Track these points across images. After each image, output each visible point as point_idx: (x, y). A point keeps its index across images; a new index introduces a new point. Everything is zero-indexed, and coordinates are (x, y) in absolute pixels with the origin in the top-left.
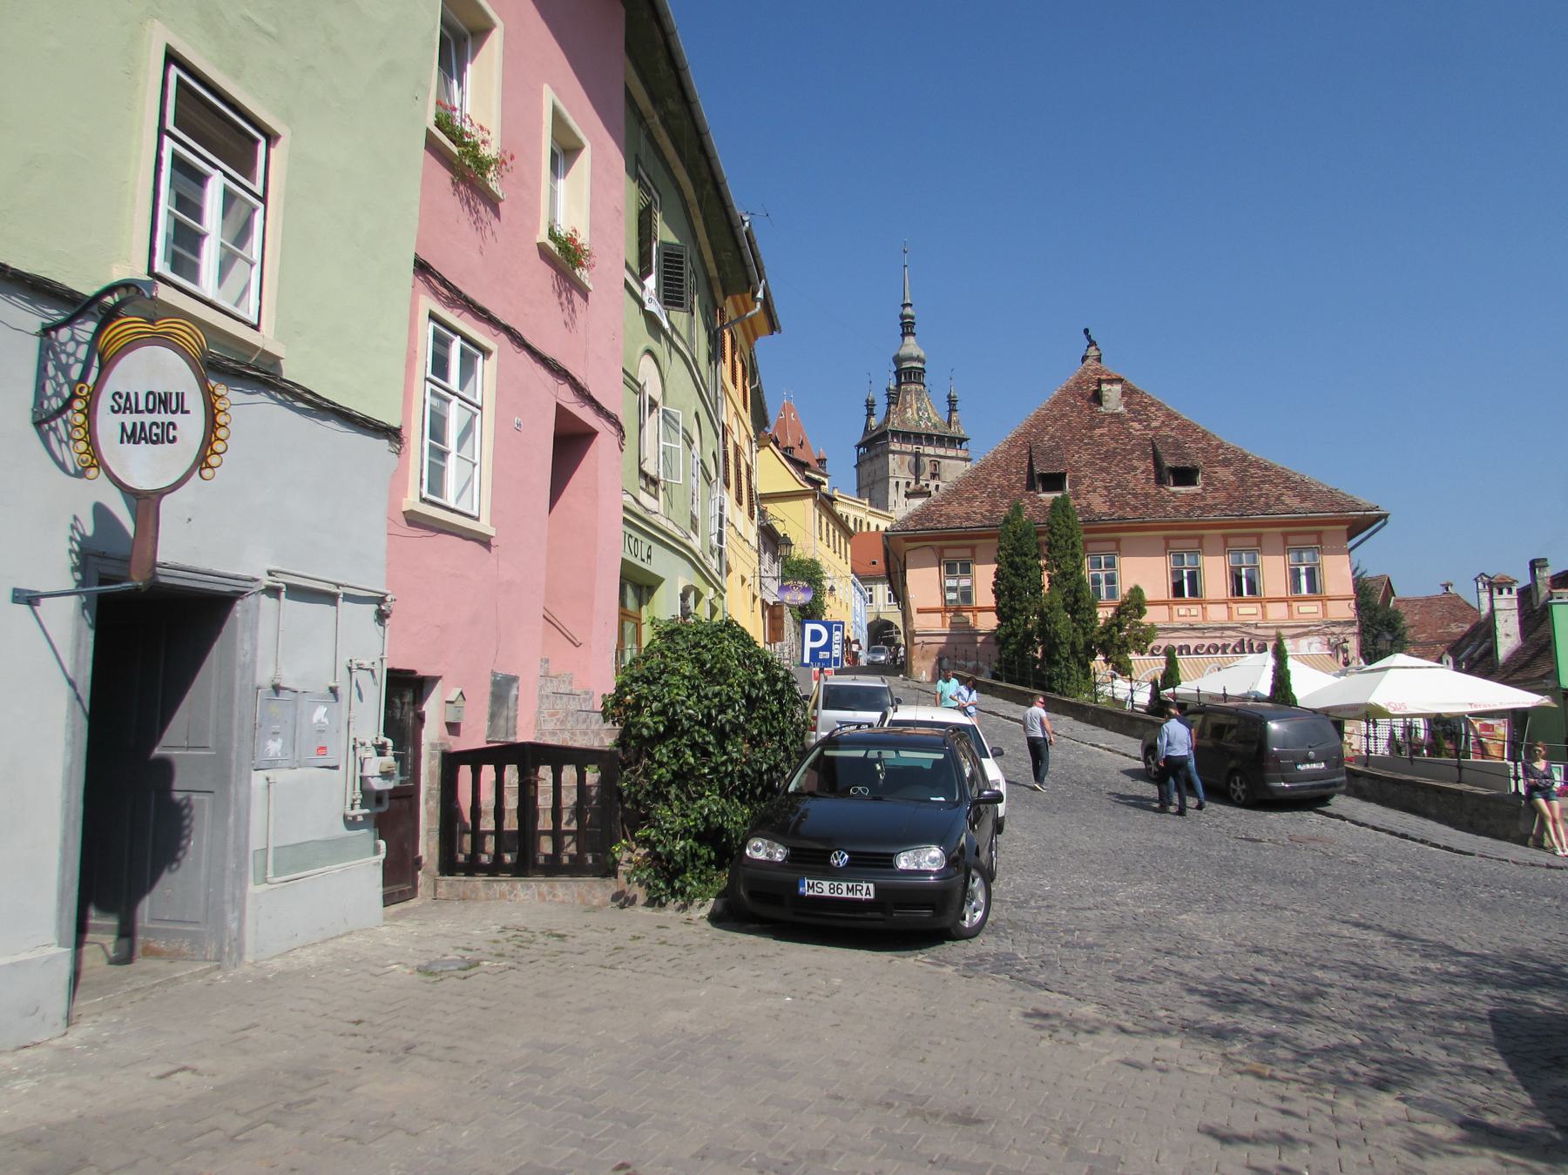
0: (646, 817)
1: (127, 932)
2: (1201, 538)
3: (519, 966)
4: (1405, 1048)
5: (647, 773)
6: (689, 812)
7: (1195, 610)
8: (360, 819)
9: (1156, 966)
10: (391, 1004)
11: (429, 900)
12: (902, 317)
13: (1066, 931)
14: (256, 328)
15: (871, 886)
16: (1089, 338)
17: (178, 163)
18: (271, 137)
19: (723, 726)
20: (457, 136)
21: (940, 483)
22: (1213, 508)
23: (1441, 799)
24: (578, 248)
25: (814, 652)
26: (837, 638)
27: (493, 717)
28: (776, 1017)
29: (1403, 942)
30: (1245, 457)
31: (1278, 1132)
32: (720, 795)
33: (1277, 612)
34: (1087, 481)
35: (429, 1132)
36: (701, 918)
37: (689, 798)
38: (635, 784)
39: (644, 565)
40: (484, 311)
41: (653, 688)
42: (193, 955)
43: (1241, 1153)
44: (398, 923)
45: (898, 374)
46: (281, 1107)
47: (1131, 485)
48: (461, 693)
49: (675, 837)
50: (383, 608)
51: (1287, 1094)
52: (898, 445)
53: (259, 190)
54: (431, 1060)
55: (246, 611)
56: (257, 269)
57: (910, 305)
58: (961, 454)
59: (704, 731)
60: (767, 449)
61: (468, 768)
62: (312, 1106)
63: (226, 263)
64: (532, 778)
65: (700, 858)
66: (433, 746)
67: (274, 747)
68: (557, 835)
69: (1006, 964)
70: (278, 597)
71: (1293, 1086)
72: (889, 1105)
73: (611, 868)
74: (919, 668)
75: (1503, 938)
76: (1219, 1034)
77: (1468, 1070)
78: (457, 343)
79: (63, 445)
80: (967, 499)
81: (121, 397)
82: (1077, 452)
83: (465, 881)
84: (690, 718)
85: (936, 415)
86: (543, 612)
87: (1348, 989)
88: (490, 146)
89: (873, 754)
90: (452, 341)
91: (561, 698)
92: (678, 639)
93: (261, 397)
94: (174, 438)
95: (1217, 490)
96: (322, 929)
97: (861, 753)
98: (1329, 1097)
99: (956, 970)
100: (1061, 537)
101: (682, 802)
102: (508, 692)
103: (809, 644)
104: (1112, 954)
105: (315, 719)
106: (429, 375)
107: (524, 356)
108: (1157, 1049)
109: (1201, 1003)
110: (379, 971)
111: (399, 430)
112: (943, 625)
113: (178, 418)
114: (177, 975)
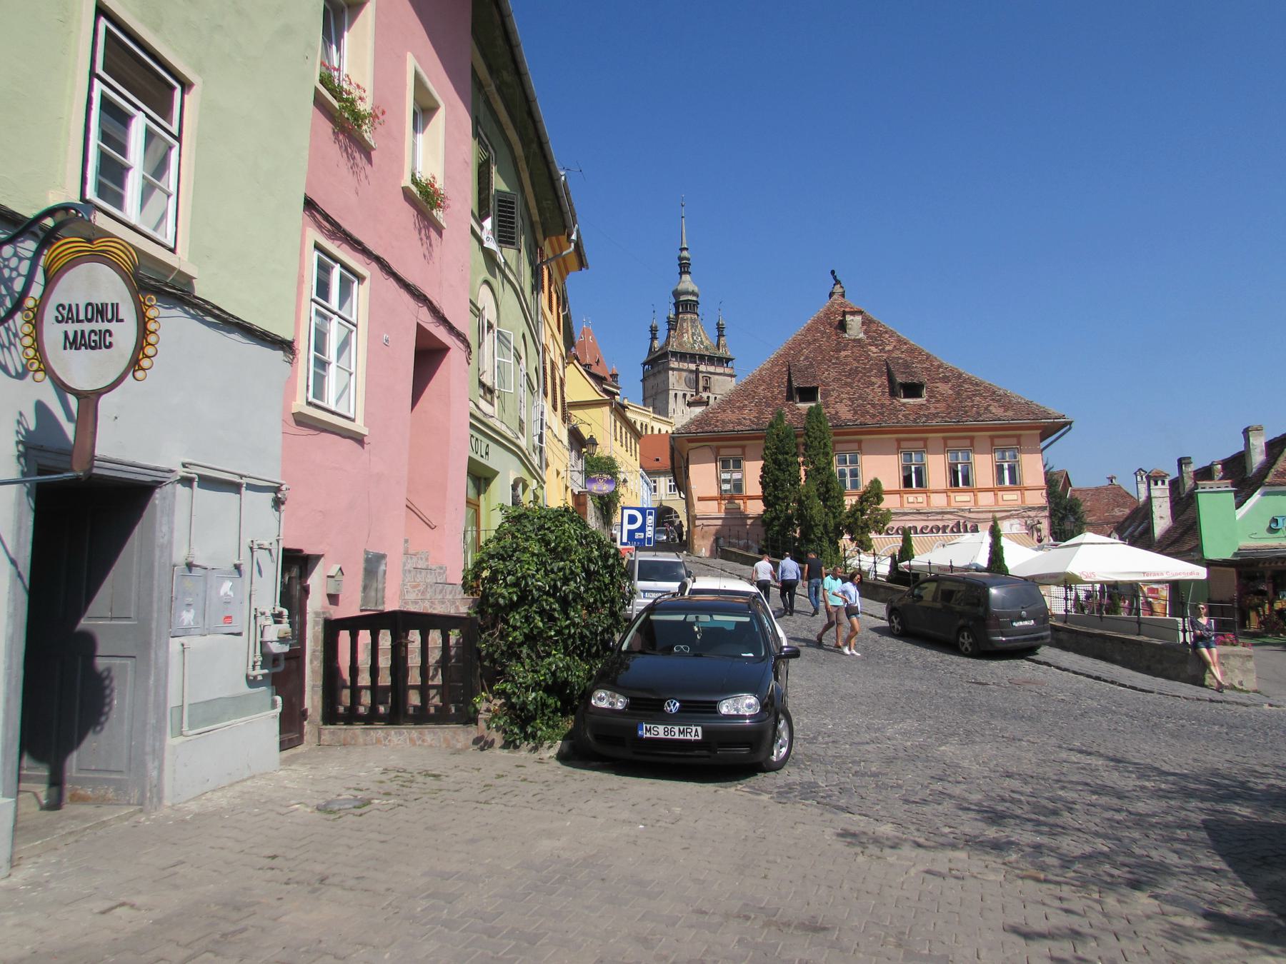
0: (502, 673)
1: (56, 781)
2: (925, 440)
3: (406, 804)
4: (1145, 853)
5: (503, 636)
6: (538, 668)
7: (921, 498)
8: (260, 678)
9: (931, 790)
10: (300, 840)
11: (314, 745)
12: (680, 259)
13: (853, 762)
14: (173, 251)
15: (699, 729)
16: (835, 278)
17: (106, 104)
18: (186, 85)
19: (566, 596)
20: (337, 92)
22: (935, 415)
23: (1125, 648)
24: (436, 191)
25: (631, 533)
26: (650, 521)
27: (365, 588)
28: (635, 843)
29: (1121, 765)
30: (960, 376)
31: (1067, 928)
32: (564, 654)
33: (986, 500)
34: (835, 394)
35: (354, 955)
36: (550, 757)
37: (539, 656)
38: (492, 645)
39: (482, 461)
40: (359, 243)
41: (507, 563)
42: (117, 800)
43: (1043, 947)
44: (293, 767)
45: (677, 305)
46: (217, 937)
47: (870, 397)
48: (340, 569)
49: (527, 689)
50: (279, 496)
51: (1063, 895)
52: (676, 363)
53: (175, 130)
54: (345, 889)
55: (164, 498)
56: (173, 200)
57: (687, 249)
58: (727, 371)
59: (551, 600)
60: (571, 365)
61: (347, 632)
62: (245, 935)
63: (148, 190)
64: (403, 641)
65: (548, 706)
66: (317, 614)
67: (188, 617)
68: (424, 689)
69: (812, 792)
70: (191, 487)
71: (1065, 888)
72: (747, 918)
73: (472, 715)
74: (699, 546)
75: (1195, 760)
76: (997, 846)
77: (1200, 870)
78: (337, 271)
79: (5, 350)
80: (739, 407)
81: (64, 309)
82: (827, 370)
83: (346, 729)
84: (539, 589)
85: (707, 339)
86: (406, 502)
87: (1088, 805)
88: (365, 102)
89: (691, 618)
90: (333, 268)
91: (420, 572)
92: (525, 522)
93: (177, 312)
94: (110, 343)
95: (938, 401)
96: (230, 774)
97: (681, 618)
98: (1096, 896)
99: (771, 798)
100: (815, 438)
101: (532, 660)
102: (377, 567)
103: (627, 527)
104: (895, 781)
105: (222, 593)
106: (314, 296)
107: (391, 282)
108: (950, 861)
109: (976, 819)
110: (284, 810)
111: (292, 343)
112: (719, 511)
113: (113, 326)
114: (105, 819)
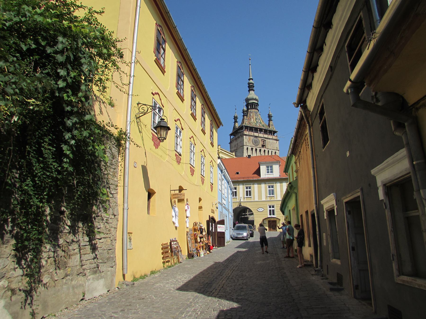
12: (249, 84)
21: (266, 149)
45: (247, 106)
52: (247, 132)
57: (252, 79)
58: (274, 137)
